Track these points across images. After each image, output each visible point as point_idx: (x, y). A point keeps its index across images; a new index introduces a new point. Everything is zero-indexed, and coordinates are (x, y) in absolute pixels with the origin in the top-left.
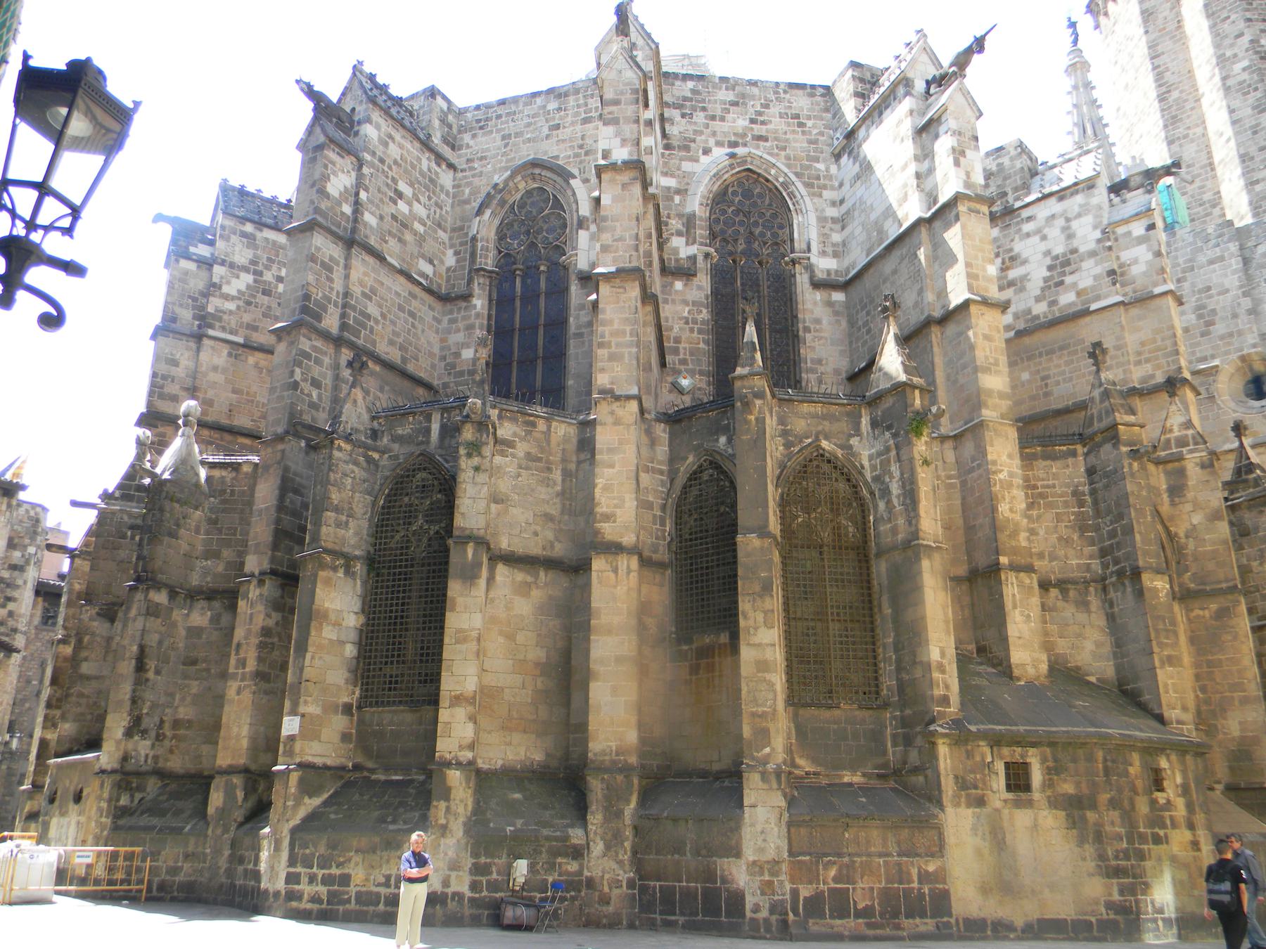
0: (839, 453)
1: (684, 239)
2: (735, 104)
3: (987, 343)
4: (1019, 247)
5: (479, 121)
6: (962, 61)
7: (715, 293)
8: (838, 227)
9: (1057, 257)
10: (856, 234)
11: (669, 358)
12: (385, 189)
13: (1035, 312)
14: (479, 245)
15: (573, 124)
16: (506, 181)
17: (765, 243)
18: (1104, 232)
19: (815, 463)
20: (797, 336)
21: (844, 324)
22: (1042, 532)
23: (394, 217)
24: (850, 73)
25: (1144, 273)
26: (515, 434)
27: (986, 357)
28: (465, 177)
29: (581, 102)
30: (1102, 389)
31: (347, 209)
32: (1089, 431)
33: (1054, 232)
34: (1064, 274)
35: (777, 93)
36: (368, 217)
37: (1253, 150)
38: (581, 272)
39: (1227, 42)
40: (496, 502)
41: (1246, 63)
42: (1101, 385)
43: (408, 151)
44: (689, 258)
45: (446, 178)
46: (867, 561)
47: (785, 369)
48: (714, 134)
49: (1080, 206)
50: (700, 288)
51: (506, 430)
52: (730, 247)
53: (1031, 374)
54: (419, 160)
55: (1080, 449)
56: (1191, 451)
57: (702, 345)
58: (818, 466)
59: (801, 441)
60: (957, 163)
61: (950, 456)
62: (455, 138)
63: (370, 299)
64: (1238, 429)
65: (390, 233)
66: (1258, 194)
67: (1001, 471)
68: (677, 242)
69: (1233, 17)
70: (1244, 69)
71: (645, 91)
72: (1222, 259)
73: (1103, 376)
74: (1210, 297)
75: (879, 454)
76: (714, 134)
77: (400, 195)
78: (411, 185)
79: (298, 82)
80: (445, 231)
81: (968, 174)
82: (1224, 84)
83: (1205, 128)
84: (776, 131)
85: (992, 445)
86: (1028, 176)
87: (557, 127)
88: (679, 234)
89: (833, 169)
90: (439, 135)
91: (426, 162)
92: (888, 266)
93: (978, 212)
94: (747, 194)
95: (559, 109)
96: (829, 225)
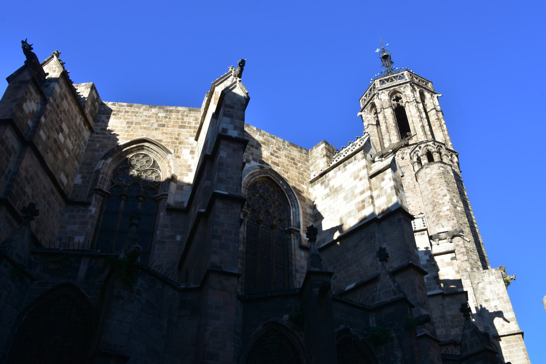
2: (264, 143)
12: (55, 122)
14: (101, 176)
15: (173, 126)
17: (275, 218)
23: (55, 141)
28: (98, 137)
29: (180, 117)
30: (472, 329)
31: (30, 123)
36: (42, 134)
38: (169, 205)
39: (439, 197)
41: (448, 207)
43: (72, 109)
45: (86, 134)
48: (252, 154)
54: (76, 117)
63: (29, 183)
65: (51, 149)
69: (442, 188)
70: (448, 210)
76: (252, 154)
77: (62, 130)
78: (69, 128)
79: (23, 42)
80: (79, 163)
84: (283, 163)
90: (89, 109)
91: (79, 120)
95: (166, 117)
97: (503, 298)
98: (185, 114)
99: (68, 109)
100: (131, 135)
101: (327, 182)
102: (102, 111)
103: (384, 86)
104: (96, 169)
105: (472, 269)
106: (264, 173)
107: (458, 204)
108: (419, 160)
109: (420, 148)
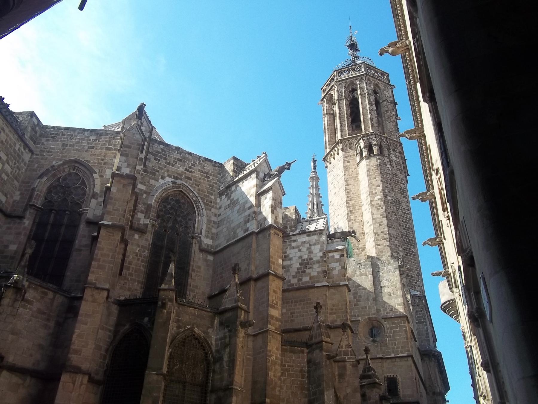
0: (202, 335)
1: (144, 215)
2: (180, 160)
3: (274, 294)
4: (289, 252)
5: (53, 134)
6: (281, 170)
7: (154, 244)
8: (216, 226)
9: (304, 260)
10: (223, 231)
11: (124, 271)
13: (292, 282)
14: (36, 193)
15: (101, 148)
16: (59, 166)
17: (182, 226)
18: (323, 254)
19: (190, 338)
20: (188, 273)
21: (211, 271)
22: (285, 388)
24: (232, 161)
25: (338, 275)
26: (34, 298)
27: (273, 300)
28: (37, 158)
29: (107, 140)
32: (310, 343)
33: (304, 249)
34: (306, 268)
35: (200, 161)
37: (379, 232)
38: (88, 219)
40: (13, 334)
41: (379, 197)
42: (318, 321)
43: (10, 139)
44: (144, 224)
45: (27, 156)
46: (206, 394)
47: (181, 288)
48: (168, 171)
49: (316, 240)
50: (146, 240)
51: (30, 295)
52: (165, 224)
53: (287, 310)
54: (15, 144)
55: (306, 350)
56: (349, 358)
57: (142, 268)
58: (191, 340)
59: (185, 327)
60: (273, 212)
61: (250, 344)
62: (37, 139)
64: (367, 351)
66: (379, 250)
67: (272, 356)
68: (140, 216)
69: (377, 178)
70: (379, 199)
71: (143, 146)
72: (365, 274)
73: (319, 318)
74: (359, 289)
75: (221, 339)
76: (168, 171)
78: (7, 155)
80: (18, 182)
81: (276, 218)
82: (371, 203)
83: (363, 218)
84: (196, 177)
85: (270, 343)
86: (297, 222)
87: (93, 148)
88: (142, 212)
89: (218, 200)
90: (29, 135)
91: (18, 146)
92: (236, 249)
93: (278, 235)
94: (177, 201)
95: (96, 140)
96: (212, 224)
97: (396, 286)
98: (113, 137)
99: (6, 140)
100: (64, 157)
101: (229, 195)
102: (42, 134)
103: (344, 77)
104: (32, 187)
105: (392, 254)
106: (177, 188)
107: (389, 194)
108: (361, 151)
109: (363, 140)
